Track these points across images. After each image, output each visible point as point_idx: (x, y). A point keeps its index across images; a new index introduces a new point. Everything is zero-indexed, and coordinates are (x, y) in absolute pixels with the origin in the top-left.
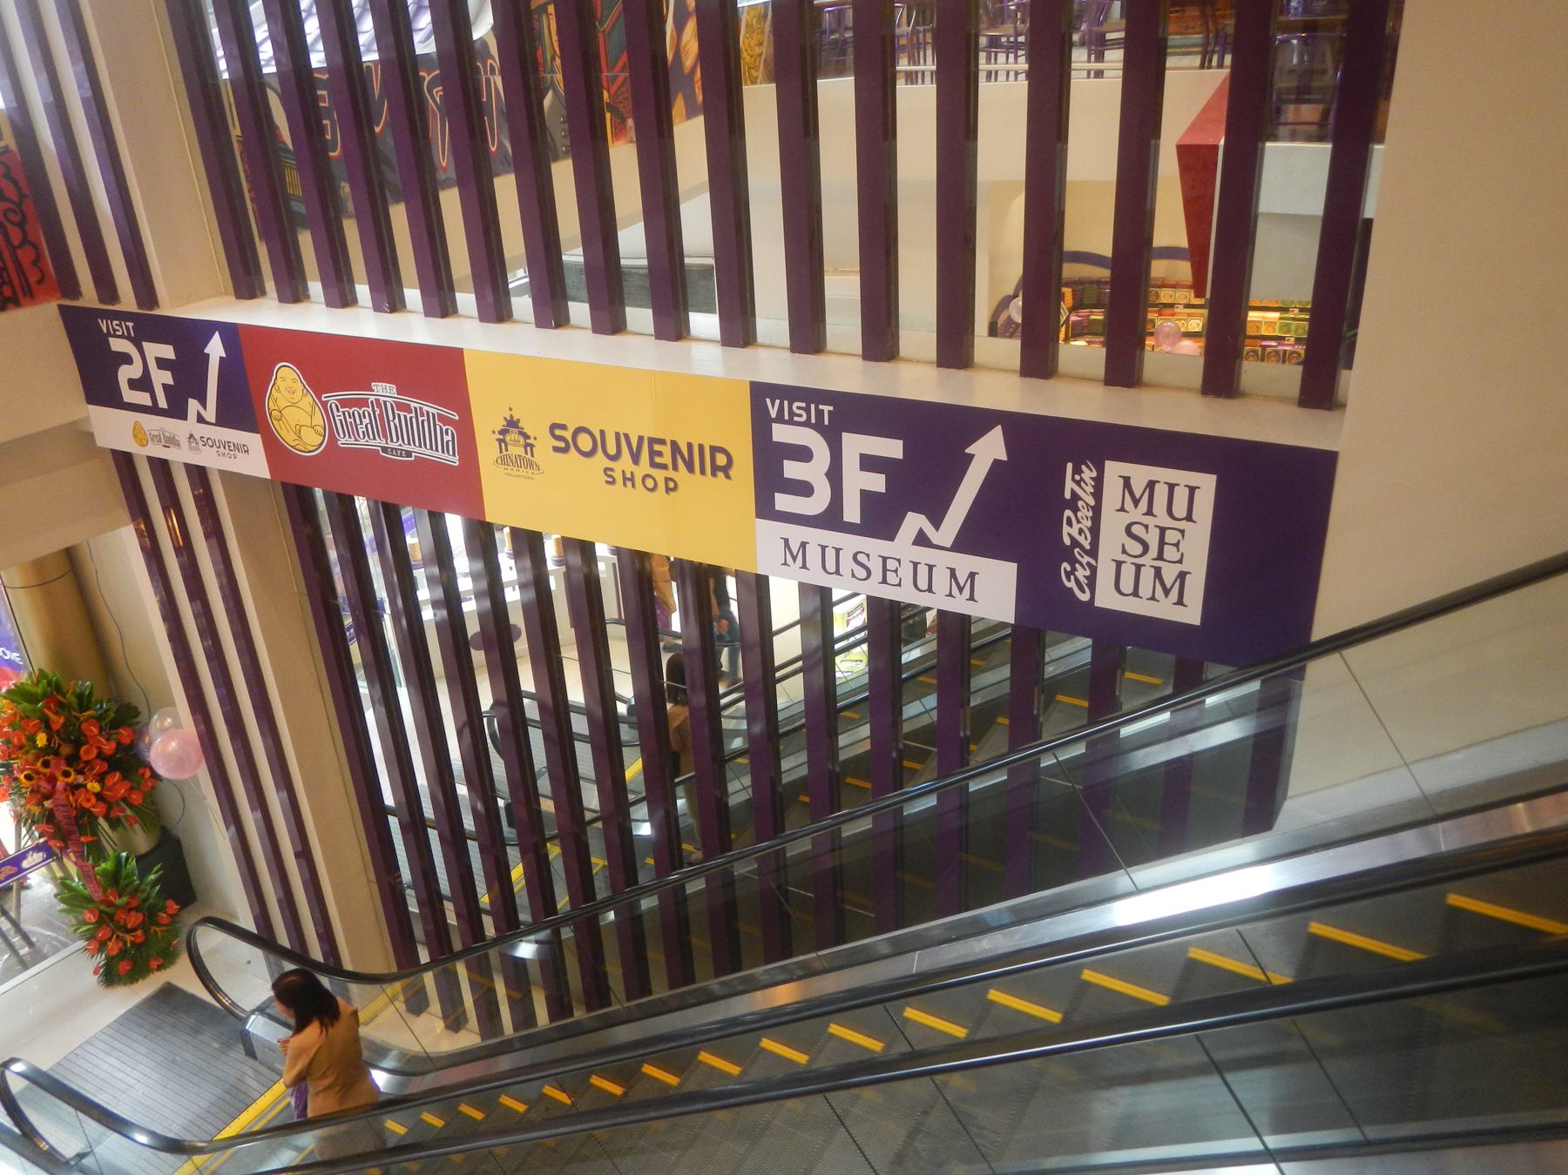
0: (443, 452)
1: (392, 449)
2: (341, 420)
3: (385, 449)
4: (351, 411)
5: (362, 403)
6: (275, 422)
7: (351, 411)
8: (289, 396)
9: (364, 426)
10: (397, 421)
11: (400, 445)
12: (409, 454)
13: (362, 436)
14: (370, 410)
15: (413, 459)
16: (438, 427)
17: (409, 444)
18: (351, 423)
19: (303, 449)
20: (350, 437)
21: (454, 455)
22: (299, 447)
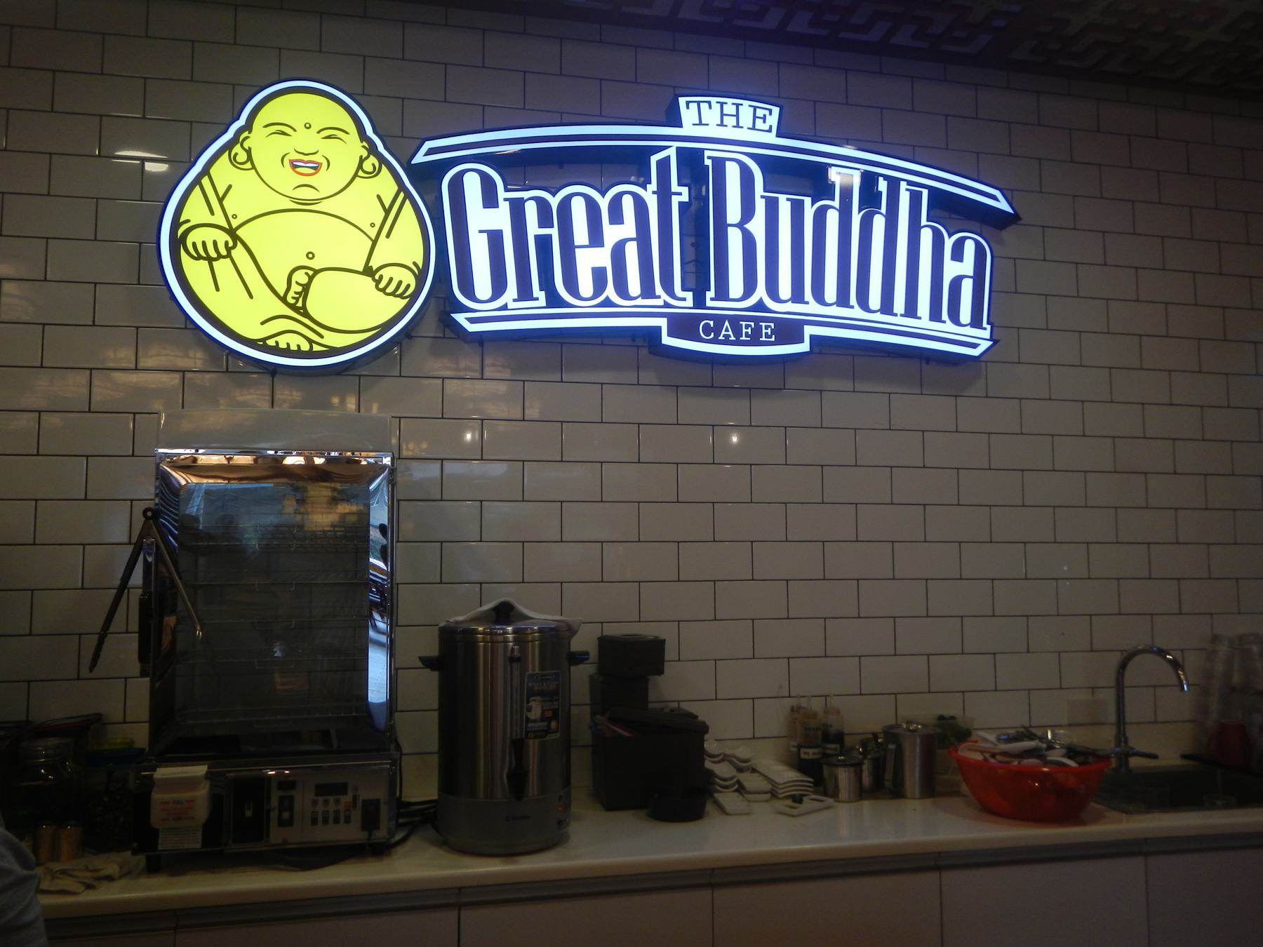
0: (935, 315)
1: (719, 320)
2: (495, 238)
3: (683, 326)
4: (554, 202)
6: (196, 271)
7: (554, 202)
8: (287, 180)
10: (757, 227)
11: (760, 306)
12: (788, 330)
13: (586, 285)
14: (650, 197)
15: (804, 347)
16: (926, 237)
17: (797, 297)
18: (544, 244)
19: (305, 347)
20: (525, 293)
21: (976, 322)
22: (283, 342)
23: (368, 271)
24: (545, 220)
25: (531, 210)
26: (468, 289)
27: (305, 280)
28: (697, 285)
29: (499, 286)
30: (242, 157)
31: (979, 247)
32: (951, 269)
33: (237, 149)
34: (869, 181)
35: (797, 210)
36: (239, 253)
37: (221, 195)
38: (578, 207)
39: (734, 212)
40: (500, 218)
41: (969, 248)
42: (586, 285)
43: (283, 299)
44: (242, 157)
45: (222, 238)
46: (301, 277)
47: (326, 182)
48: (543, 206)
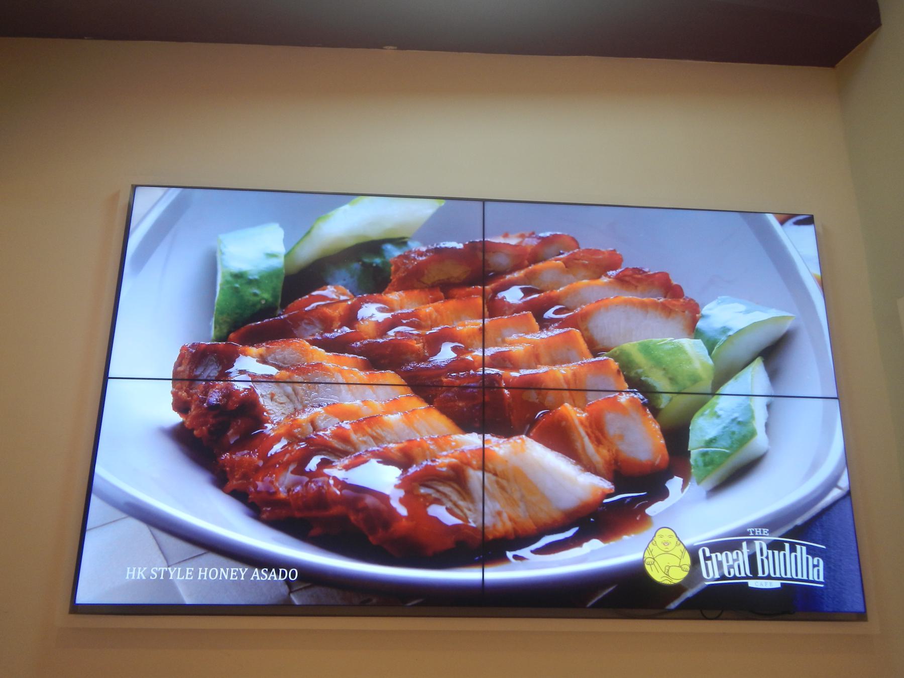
8: (663, 547)
23: (680, 566)
27: (668, 569)
30: (654, 543)
33: (653, 541)
36: (655, 563)
37: (651, 550)
43: (664, 573)
44: (654, 543)
45: (652, 560)
46: (667, 568)
47: (670, 547)
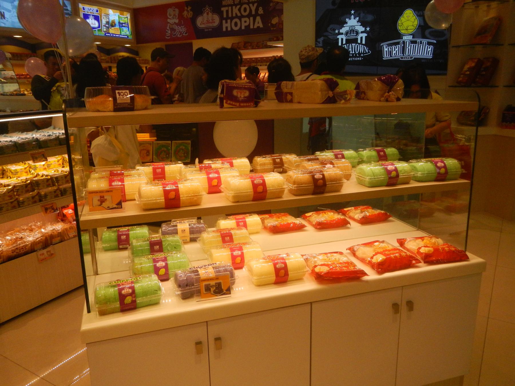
2: (386, 51)
5: (398, 43)
9: (395, 51)
10: (409, 48)
11: (409, 55)
13: (393, 54)
24: (390, 49)
25: (389, 48)
26: (384, 56)
28: (403, 53)
29: (386, 55)
31: (432, 47)
32: (429, 50)
34: (421, 41)
35: (414, 46)
38: (393, 48)
39: (407, 46)
40: (387, 49)
41: (431, 48)
42: (393, 54)
48: (390, 48)
